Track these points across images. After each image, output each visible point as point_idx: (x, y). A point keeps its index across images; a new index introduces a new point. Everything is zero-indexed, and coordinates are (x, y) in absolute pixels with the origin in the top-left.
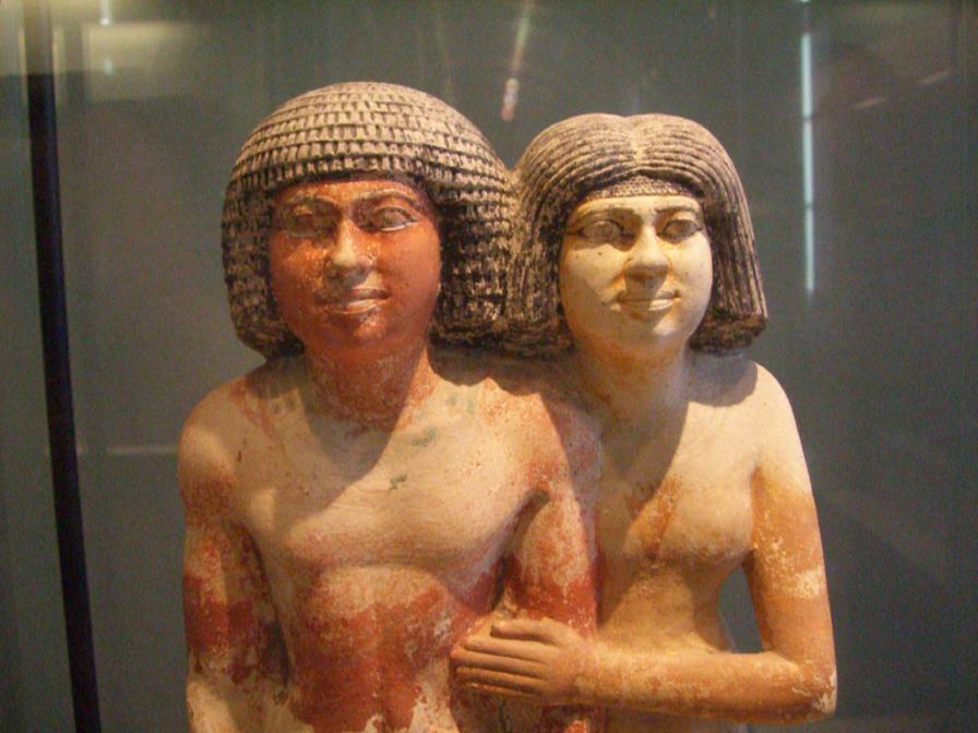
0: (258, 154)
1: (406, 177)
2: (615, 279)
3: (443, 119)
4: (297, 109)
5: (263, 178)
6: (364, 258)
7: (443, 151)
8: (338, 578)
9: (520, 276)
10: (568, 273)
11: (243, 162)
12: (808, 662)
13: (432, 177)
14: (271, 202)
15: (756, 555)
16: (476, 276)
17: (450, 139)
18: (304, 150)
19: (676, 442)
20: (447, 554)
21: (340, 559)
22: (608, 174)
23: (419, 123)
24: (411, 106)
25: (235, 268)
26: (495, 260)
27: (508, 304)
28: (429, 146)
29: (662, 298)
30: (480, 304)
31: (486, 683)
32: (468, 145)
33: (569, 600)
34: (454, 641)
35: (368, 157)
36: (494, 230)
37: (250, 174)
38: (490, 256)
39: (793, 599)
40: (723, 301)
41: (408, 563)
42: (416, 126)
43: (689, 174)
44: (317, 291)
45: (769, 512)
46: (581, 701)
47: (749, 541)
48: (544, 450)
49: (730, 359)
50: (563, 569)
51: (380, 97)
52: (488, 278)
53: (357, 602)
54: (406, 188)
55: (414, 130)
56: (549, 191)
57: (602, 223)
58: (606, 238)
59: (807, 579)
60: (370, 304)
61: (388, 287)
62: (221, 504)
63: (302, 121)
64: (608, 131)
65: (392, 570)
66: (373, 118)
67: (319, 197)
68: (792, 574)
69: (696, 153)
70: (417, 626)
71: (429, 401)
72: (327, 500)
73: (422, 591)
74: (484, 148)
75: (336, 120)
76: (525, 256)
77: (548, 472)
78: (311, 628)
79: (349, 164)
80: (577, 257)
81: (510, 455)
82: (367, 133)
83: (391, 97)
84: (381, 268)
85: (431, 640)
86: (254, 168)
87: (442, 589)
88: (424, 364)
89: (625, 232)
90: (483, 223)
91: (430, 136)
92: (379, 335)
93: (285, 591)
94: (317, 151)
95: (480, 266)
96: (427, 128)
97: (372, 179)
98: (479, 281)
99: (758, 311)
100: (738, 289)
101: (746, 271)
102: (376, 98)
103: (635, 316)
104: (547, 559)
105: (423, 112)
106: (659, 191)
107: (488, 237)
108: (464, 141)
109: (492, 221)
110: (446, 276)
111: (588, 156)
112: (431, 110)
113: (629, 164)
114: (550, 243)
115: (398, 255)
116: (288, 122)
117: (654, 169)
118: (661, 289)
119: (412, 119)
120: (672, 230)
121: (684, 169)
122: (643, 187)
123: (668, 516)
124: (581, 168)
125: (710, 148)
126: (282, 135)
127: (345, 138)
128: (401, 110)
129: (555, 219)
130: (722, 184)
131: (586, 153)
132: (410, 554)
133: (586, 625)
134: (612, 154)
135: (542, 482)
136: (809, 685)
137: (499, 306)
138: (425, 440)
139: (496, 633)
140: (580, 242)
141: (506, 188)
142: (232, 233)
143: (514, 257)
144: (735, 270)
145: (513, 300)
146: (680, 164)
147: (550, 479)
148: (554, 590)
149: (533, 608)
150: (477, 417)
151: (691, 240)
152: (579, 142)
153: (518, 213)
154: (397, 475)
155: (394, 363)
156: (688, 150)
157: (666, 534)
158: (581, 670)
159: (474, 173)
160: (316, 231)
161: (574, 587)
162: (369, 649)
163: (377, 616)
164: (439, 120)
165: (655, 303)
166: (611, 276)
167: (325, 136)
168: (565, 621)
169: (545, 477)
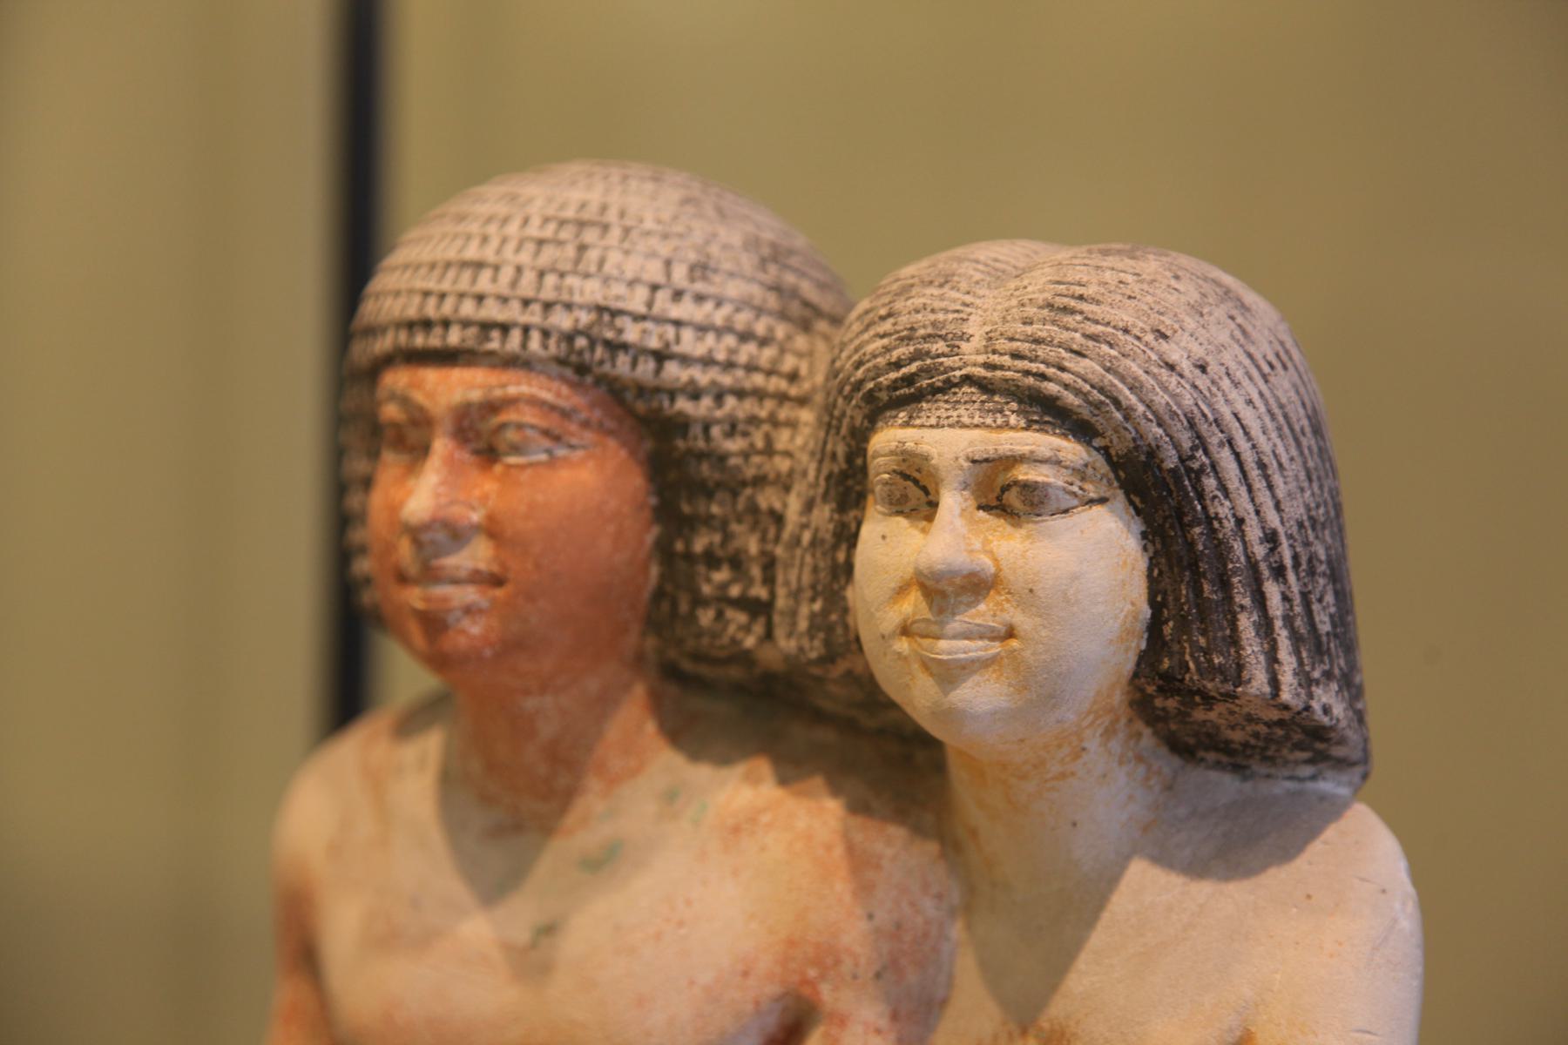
1: (555, 369)
2: (901, 591)
7: (638, 318)
22: (909, 380)
23: (601, 262)
27: (777, 618)
29: (967, 636)
30: (720, 615)
35: (486, 327)
36: (750, 472)
38: (739, 520)
40: (1171, 657)
42: (593, 269)
43: (1052, 388)
49: (1282, 787)
54: (556, 385)
55: (587, 276)
60: (470, 594)
79: (454, 337)
90: (723, 458)
92: (488, 653)
96: (615, 272)
97: (493, 366)
101: (1229, 598)
106: (989, 421)
107: (734, 486)
109: (746, 455)
110: (664, 550)
114: (842, 507)
117: (989, 374)
119: (593, 255)
120: (1012, 498)
121: (1043, 377)
124: (869, 365)
129: (850, 458)
134: (926, 338)
135: (805, 982)
137: (762, 620)
144: (1198, 591)
146: (1034, 367)
147: (823, 977)
156: (1065, 335)
159: (708, 361)
165: (943, 644)
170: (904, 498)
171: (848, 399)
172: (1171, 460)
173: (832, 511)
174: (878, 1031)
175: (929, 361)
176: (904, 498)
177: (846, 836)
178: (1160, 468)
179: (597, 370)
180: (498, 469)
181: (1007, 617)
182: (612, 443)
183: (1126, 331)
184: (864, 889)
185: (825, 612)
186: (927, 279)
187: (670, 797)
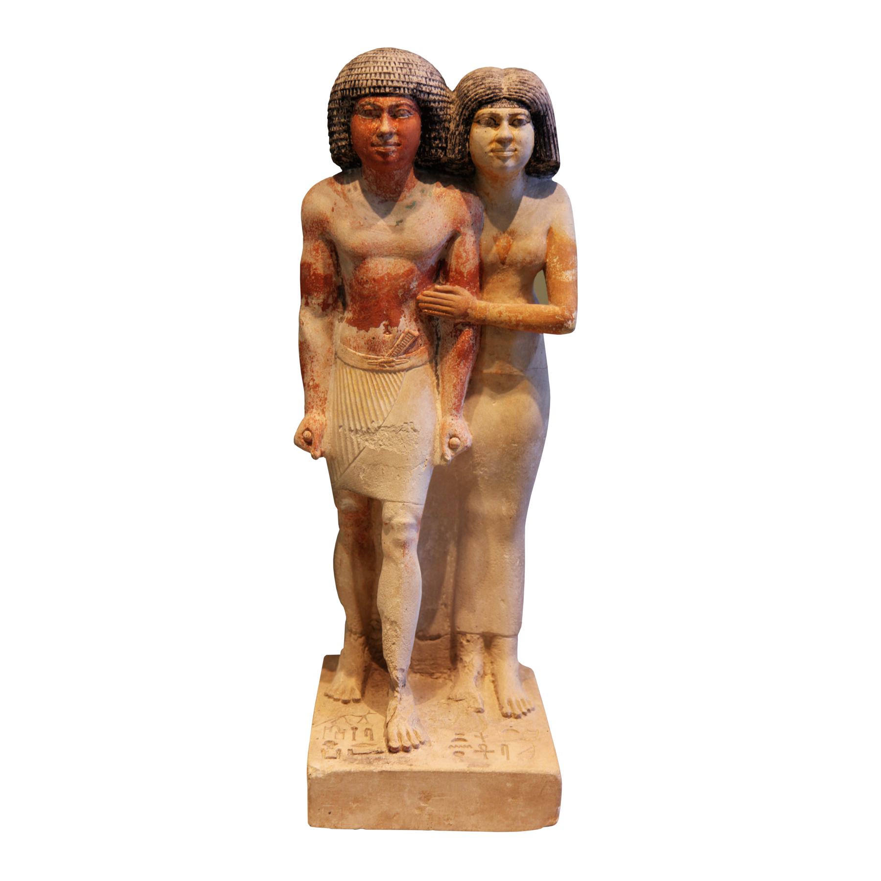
0: (349, 81)
1: (409, 97)
2: (491, 142)
3: (425, 70)
4: (365, 62)
5: (351, 92)
6: (392, 129)
7: (424, 85)
8: (373, 262)
9: (453, 139)
10: (473, 139)
11: (341, 83)
12: (563, 306)
13: (420, 97)
14: (354, 102)
15: (547, 264)
16: (435, 138)
17: (428, 80)
18: (369, 83)
19: (515, 214)
20: (418, 253)
21: (374, 254)
22: (491, 98)
24: (412, 64)
25: (335, 128)
26: (444, 132)
27: (447, 151)
28: (419, 83)
29: (509, 151)
30: (436, 151)
31: (431, 310)
32: (435, 82)
33: (467, 278)
34: (418, 292)
35: (395, 88)
36: (444, 119)
37: (345, 89)
39: (560, 282)
40: (538, 153)
41: (402, 257)
43: (524, 99)
44: (373, 141)
45: (554, 246)
46: (469, 321)
47: (545, 258)
48: (459, 214)
49: (546, 180)
50: (465, 265)
51: (400, 60)
52: (440, 139)
53: (380, 272)
54: (409, 100)
55: (413, 76)
56: (467, 103)
57: (487, 119)
58: (488, 124)
59: (567, 274)
60: (393, 148)
61: (401, 141)
62: (323, 230)
63: (368, 69)
64: (493, 78)
65: (395, 259)
66: (397, 70)
67: (375, 103)
68: (561, 272)
69: (528, 90)
70: (404, 283)
71: (413, 191)
72: (370, 226)
73: (407, 269)
74: (441, 82)
75: (382, 70)
76: (456, 131)
77: (460, 223)
78: (360, 283)
79: (387, 90)
80: (477, 132)
81: (445, 215)
82: (395, 77)
83: (404, 59)
84: (398, 134)
85: (409, 290)
86: (347, 87)
87: (416, 268)
88: (411, 176)
89: (496, 123)
90: (439, 116)
91: (420, 79)
92: (396, 161)
93: (347, 269)
94: (374, 84)
95: (437, 134)
96: (419, 75)
97: (397, 97)
98: (436, 141)
99: (554, 158)
100: (545, 148)
101: (549, 141)
102: (398, 60)
103: (499, 158)
104: (459, 260)
105: (417, 67)
107: (441, 121)
108: (433, 80)
109: (443, 115)
110: (423, 137)
111: (483, 90)
112: (420, 66)
113: (500, 94)
114: (466, 126)
115: (405, 128)
116: (362, 68)
117: (510, 97)
118: (509, 147)
119: (413, 71)
120: (516, 123)
121: (522, 97)
122: (505, 104)
123: (510, 245)
125: (535, 87)
126: (360, 74)
127: (386, 79)
128: (408, 66)
129: (469, 115)
130: (539, 103)
131: (483, 89)
132: (402, 253)
133: (474, 291)
134: (494, 89)
135: (458, 227)
136: (563, 316)
138: (412, 206)
139: (437, 290)
140: (479, 126)
141: (450, 100)
142: (335, 113)
143: (451, 131)
144: (544, 140)
145: (450, 149)
146: (521, 95)
147: (461, 226)
148: (461, 273)
149: (452, 282)
150: (433, 199)
151: (524, 127)
152: (480, 83)
153: (454, 112)
154: (399, 220)
155: (401, 173)
156: (525, 88)
157: (509, 253)
158: (470, 306)
159: (437, 95)
160: (373, 116)
161: (469, 273)
162: (384, 292)
163: (388, 279)
164: (423, 71)
165: (505, 153)
166: (489, 141)
167: (378, 77)
169: (459, 225)
170: (490, 123)
171: (473, 102)
172: (542, 114)
173: (464, 127)
174: (472, 236)
175: (495, 94)
176: (490, 123)
177: (462, 196)
178: (540, 115)
179: (417, 97)
180: (397, 120)
181: (515, 147)
182: (417, 113)
183: (535, 87)
184: (469, 207)
185: (462, 149)
186: (488, 76)
187: (423, 191)
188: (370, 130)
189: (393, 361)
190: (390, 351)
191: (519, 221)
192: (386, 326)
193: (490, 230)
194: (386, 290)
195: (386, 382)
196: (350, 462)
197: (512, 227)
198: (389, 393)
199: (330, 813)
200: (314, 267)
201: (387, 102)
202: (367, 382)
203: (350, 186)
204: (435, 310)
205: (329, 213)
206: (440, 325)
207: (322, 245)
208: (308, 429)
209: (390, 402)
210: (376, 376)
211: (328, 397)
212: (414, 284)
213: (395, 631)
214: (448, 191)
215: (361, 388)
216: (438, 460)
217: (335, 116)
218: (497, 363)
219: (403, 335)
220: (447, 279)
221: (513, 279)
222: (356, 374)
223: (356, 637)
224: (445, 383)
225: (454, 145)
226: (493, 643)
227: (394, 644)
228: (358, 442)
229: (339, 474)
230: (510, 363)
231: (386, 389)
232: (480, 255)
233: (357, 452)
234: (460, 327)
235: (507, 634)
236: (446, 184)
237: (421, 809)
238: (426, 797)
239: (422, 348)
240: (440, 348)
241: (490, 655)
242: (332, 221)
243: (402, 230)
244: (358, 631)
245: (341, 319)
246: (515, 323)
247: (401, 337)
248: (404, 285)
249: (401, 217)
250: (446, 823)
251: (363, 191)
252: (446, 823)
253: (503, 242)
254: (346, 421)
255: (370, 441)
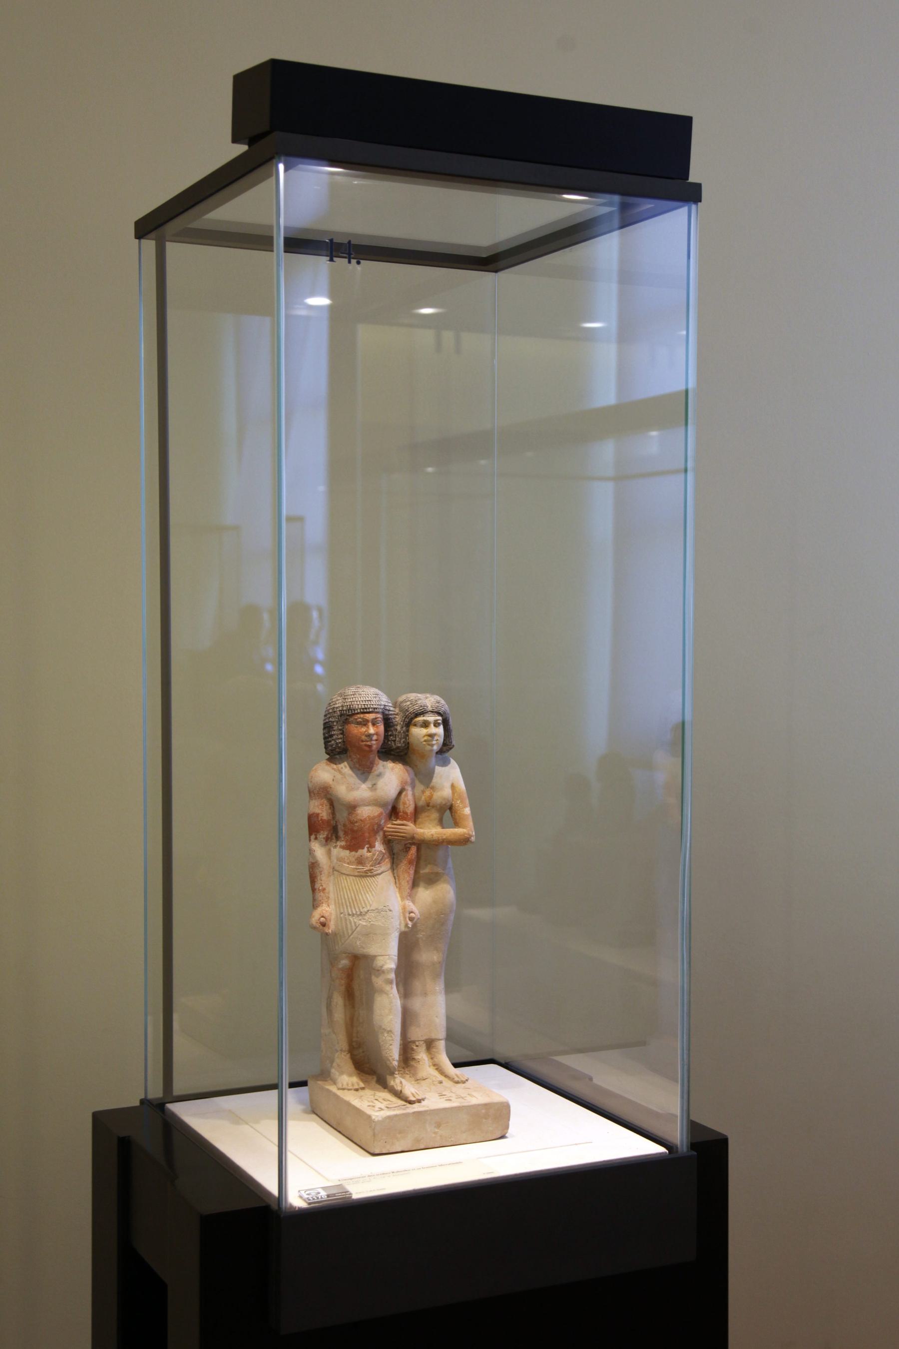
2: (424, 736)
11: (339, 707)
14: (348, 717)
15: (453, 805)
16: (391, 735)
18: (360, 706)
22: (422, 712)
35: (374, 708)
58: (422, 726)
60: (374, 742)
72: (358, 789)
73: (379, 812)
77: (405, 783)
79: (371, 710)
85: (380, 825)
86: (344, 709)
94: (363, 707)
103: (429, 745)
120: (437, 725)
123: (432, 795)
129: (409, 721)
136: (469, 834)
138: (380, 775)
139: (395, 824)
140: (415, 727)
141: (396, 713)
142: (335, 724)
148: (406, 813)
154: (373, 783)
161: (411, 813)
166: (423, 736)
168: (409, 821)
188: (361, 733)
189: (372, 869)
190: (371, 863)
191: (436, 780)
192: (368, 848)
193: (420, 787)
194: (367, 826)
195: (369, 882)
196: (350, 934)
197: (432, 784)
198: (371, 889)
199: (386, 1142)
200: (321, 815)
201: (371, 716)
202: (358, 884)
203: (342, 765)
204: (396, 836)
205: (331, 782)
206: (394, 845)
207: (326, 802)
208: (323, 917)
209: (373, 895)
210: (363, 879)
211: (330, 896)
212: (383, 821)
213: (391, 1037)
214: (396, 765)
215: (354, 888)
216: (403, 929)
217: (335, 726)
218: (429, 866)
219: (378, 853)
220: (397, 818)
221: (435, 815)
222: (349, 879)
223: (345, 1054)
224: (401, 881)
225: (401, 739)
226: (432, 1046)
227: (391, 1045)
228: (354, 921)
229: (340, 944)
230: (436, 865)
231: (370, 887)
232: (415, 802)
233: (354, 928)
234: (408, 845)
235: (440, 1038)
236: (394, 761)
237: (435, 1133)
238: (438, 1125)
239: (387, 860)
240: (395, 860)
241: (430, 1053)
242: (333, 786)
243: (376, 789)
244: (347, 1050)
245: (335, 847)
246: (441, 840)
247: (377, 854)
248: (378, 822)
249: (374, 782)
250: (450, 1140)
251: (351, 768)
252: (450, 1140)
253: (428, 793)
254: (346, 909)
255: (363, 920)
